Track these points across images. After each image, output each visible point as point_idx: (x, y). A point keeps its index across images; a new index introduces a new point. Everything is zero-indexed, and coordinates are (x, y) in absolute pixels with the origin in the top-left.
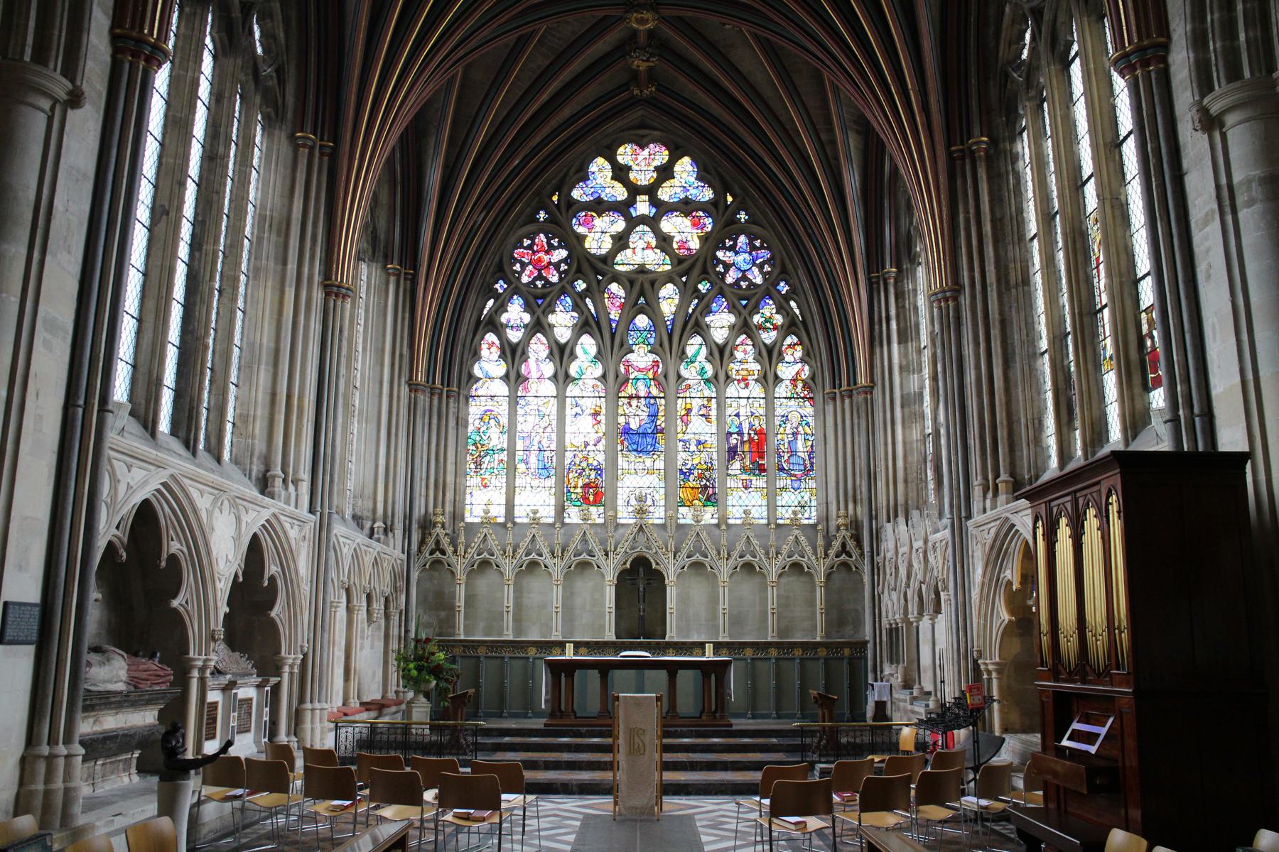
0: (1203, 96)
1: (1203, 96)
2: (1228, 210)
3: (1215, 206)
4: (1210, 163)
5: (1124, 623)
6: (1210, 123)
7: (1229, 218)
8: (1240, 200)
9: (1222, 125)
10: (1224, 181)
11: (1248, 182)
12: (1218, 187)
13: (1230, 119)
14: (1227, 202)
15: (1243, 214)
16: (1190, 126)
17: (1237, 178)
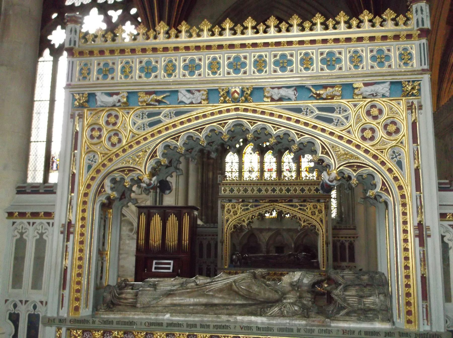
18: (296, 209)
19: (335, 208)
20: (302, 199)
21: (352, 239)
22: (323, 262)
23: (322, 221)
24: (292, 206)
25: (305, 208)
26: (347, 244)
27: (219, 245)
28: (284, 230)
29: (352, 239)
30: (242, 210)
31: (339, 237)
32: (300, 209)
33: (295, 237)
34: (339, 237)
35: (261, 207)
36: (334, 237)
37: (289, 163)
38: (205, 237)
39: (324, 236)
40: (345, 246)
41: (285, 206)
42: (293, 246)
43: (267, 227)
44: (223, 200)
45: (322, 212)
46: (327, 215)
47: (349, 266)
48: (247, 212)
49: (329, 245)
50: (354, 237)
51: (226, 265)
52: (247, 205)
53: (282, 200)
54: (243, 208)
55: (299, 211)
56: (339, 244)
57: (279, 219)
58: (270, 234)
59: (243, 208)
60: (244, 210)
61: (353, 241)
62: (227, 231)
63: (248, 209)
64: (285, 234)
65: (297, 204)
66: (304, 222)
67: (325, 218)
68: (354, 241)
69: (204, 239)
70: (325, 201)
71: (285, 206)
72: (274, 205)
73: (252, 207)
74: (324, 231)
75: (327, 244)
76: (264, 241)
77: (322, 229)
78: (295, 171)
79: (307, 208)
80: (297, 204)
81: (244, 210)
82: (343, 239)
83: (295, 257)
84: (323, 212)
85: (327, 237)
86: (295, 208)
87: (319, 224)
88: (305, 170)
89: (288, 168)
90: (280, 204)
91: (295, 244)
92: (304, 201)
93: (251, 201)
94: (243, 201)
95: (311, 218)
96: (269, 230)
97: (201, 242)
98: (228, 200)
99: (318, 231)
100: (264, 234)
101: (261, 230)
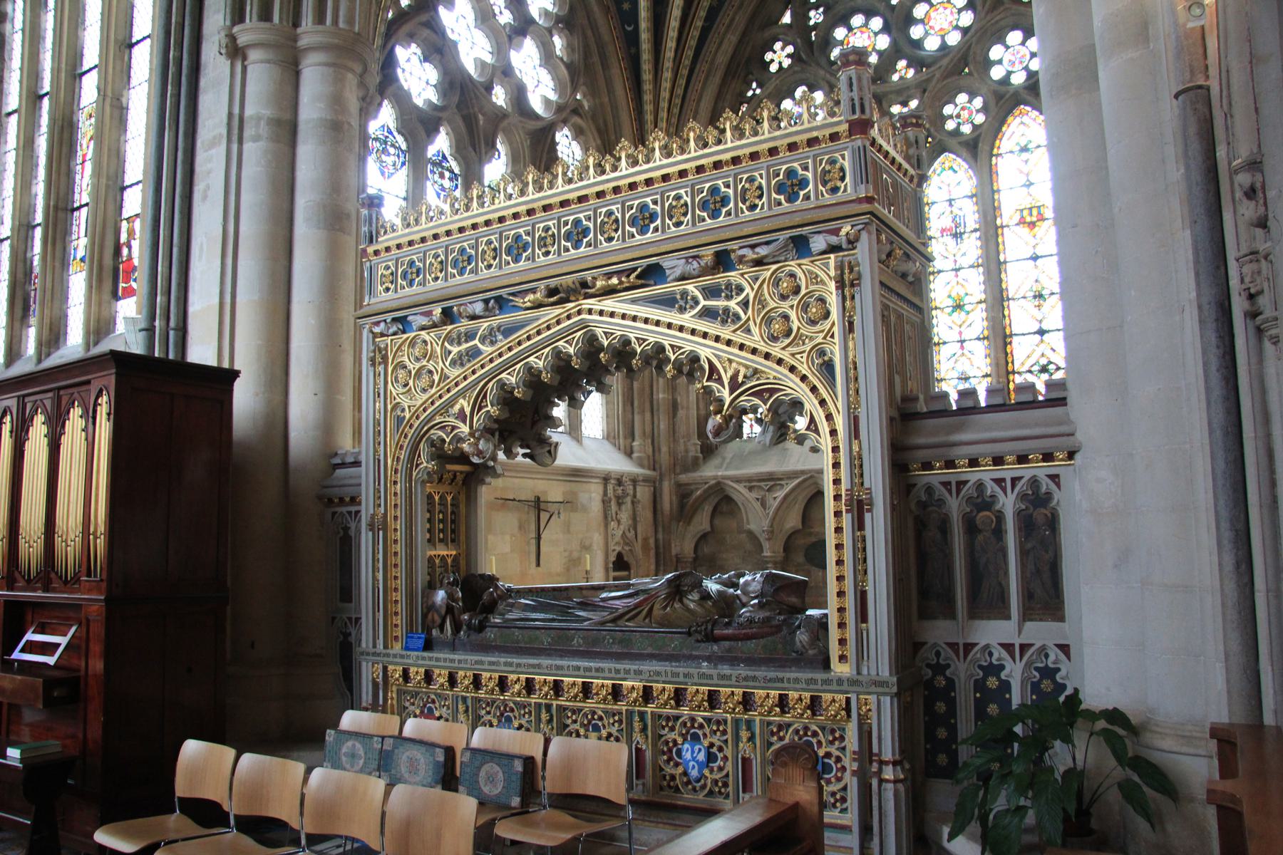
0: (234, 24)
1: (234, 24)
2: (235, 138)
3: (225, 132)
4: (227, 89)
5: (102, 528)
6: (235, 52)
7: (235, 147)
8: (248, 133)
9: (244, 58)
10: (236, 111)
11: (259, 118)
12: (230, 115)
13: (253, 55)
14: (236, 131)
15: (247, 146)
16: (216, 48)
17: (249, 112)
18: (687, 319)
19: (980, 302)
20: (708, 254)
21: (1039, 470)
23: (828, 367)
24: (667, 302)
25: (733, 304)
26: (1008, 504)
27: (366, 538)
29: (1039, 470)
30: (453, 363)
31: (950, 464)
32: (708, 314)
37: (950, 201)
40: (1000, 517)
41: (632, 310)
44: (377, 324)
45: (827, 315)
47: (1024, 648)
50: (1048, 457)
52: (470, 336)
53: (609, 276)
55: (702, 326)
59: (455, 350)
61: (1046, 484)
65: (691, 288)
66: (734, 385)
68: (1054, 478)
69: (350, 513)
70: (834, 240)
71: (632, 310)
72: (579, 312)
73: (489, 338)
74: (840, 422)
78: (975, 230)
80: (691, 288)
81: (459, 361)
82: (986, 473)
84: (835, 315)
85: (857, 464)
86: (682, 310)
88: (1017, 218)
89: (947, 222)
90: (609, 304)
92: (723, 261)
93: (478, 308)
94: (448, 316)
95: (767, 356)
97: (346, 529)
98: (394, 320)
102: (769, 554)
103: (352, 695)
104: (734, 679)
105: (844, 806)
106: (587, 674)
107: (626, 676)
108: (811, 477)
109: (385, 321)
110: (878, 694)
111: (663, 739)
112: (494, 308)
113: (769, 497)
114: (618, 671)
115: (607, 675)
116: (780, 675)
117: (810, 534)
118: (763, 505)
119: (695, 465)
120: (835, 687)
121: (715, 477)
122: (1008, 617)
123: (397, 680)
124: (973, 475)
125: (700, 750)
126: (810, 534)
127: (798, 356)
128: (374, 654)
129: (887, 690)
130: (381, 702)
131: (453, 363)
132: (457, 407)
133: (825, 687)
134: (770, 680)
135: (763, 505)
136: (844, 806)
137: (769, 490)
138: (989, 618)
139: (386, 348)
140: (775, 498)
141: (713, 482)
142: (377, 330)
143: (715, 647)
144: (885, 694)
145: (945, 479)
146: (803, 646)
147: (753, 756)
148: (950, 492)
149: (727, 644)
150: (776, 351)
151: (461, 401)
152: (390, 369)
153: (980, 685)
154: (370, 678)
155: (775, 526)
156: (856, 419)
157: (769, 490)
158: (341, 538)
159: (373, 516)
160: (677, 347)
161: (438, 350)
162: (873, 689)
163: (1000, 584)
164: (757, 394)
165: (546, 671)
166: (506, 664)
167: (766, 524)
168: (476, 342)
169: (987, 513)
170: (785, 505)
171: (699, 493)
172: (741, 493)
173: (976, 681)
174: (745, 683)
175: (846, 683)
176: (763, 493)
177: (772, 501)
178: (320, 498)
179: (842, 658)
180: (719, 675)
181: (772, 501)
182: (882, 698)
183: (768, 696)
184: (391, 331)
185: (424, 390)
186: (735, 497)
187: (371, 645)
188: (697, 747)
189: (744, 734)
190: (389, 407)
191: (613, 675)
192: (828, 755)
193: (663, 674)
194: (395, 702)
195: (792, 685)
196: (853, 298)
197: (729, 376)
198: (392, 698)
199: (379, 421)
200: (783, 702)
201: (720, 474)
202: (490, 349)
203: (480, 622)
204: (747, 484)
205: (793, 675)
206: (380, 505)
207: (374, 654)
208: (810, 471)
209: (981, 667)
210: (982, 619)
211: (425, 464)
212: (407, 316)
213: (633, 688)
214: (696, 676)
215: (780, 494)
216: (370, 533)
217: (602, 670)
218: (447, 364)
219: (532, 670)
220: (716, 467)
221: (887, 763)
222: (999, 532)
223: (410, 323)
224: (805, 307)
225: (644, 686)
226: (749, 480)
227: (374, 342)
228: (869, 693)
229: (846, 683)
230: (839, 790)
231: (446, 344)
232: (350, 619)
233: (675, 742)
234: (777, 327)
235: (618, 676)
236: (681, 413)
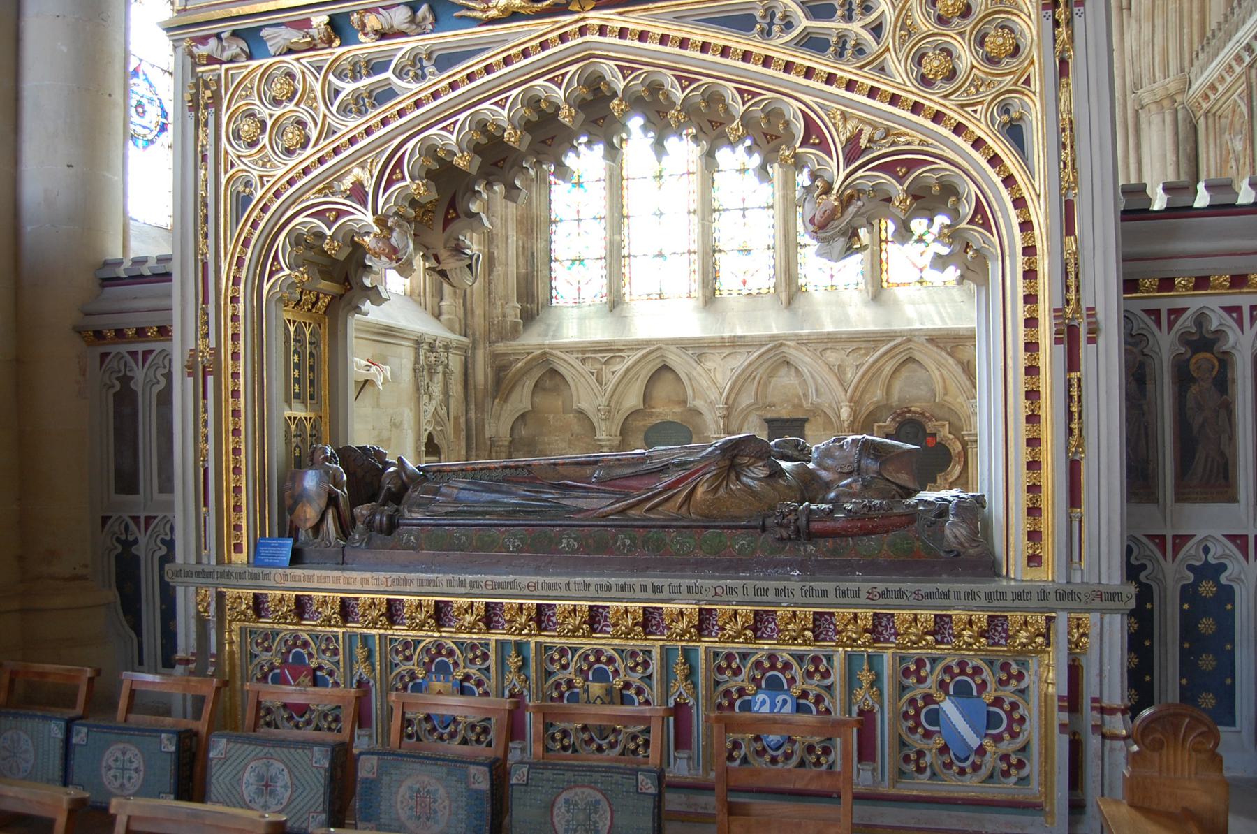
18: (778, 47)
22: (1034, 511)
27: (183, 390)
28: (802, 342)
32: (812, 43)
33: (852, 376)
34: (1167, 284)
35: (476, 64)
36: (1130, 285)
38: (141, 347)
39: (1044, 266)
40: (1225, 361)
42: (845, 413)
43: (727, 334)
44: (203, 40)
46: (1063, 68)
48: (373, 117)
49: (1086, 350)
51: (238, 548)
52: (375, 66)
54: (348, 87)
55: (804, 59)
56: (1166, 344)
57: (783, 296)
58: (740, 361)
59: (348, 87)
60: (357, 105)
62: (236, 281)
63: (384, 95)
64: (805, 359)
66: (853, 151)
67: (1053, 105)
69: (134, 354)
72: (582, 31)
73: (415, 67)
74: (1038, 213)
75: (1069, 337)
76: (713, 394)
77: (1019, 203)
79: (877, 30)
81: (357, 105)
82: (1212, 303)
83: (777, 473)
85: (1069, 275)
87: (995, 160)
91: (855, 402)
96: (735, 344)
97: (126, 380)
98: (235, 34)
99: (976, 234)
100: (709, 365)
101: (698, 349)
102: (604, 437)
103: (139, 633)
104: (863, 595)
105: (1024, 773)
106: (603, 594)
107: (673, 596)
108: (660, 348)
109: (218, 36)
110: (1103, 612)
111: (722, 688)
112: (424, 19)
113: (607, 371)
114: (658, 589)
115: (639, 595)
116: (943, 587)
117: (651, 415)
118: (600, 381)
119: (514, 332)
120: (1034, 603)
121: (541, 346)
122: (1234, 499)
123: (243, 613)
124: (1195, 303)
125: (785, 702)
126: (651, 415)
127: (969, 109)
128: (200, 574)
129: (1120, 605)
130: (214, 650)
131: (344, 110)
132: (347, 183)
133: (1018, 603)
134: (926, 596)
135: (600, 381)
136: (1024, 773)
137: (606, 363)
138: (1205, 500)
139: (218, 81)
140: (613, 372)
141: (538, 352)
142: (202, 50)
143: (811, 547)
144: (1112, 611)
145: (1152, 305)
146: (961, 544)
147: (877, 708)
148: (1158, 323)
149: (830, 543)
150: (932, 101)
151: (357, 171)
152: (224, 119)
153: (1188, 593)
154: (193, 612)
155: (613, 404)
156: (1069, 206)
157: (606, 363)
158: (115, 394)
159: (194, 352)
160: (749, 92)
161: (317, 87)
162: (1097, 604)
163: (1222, 454)
164: (887, 168)
165: (527, 592)
166: (451, 583)
167: (602, 402)
168: (389, 74)
169: (1208, 355)
170: (625, 381)
171: (520, 364)
172: (570, 368)
173: (1184, 587)
174: (882, 601)
175: (1052, 597)
176: (598, 366)
177: (609, 376)
178: (79, 331)
179: (1034, 560)
180: (837, 589)
181: (609, 376)
182: (1107, 617)
183: (915, 619)
184: (227, 55)
185: (289, 152)
186: (562, 370)
187: (193, 560)
188: (780, 698)
189: (865, 676)
190: (224, 179)
191: (650, 595)
192: (998, 701)
193: (740, 591)
194: (235, 648)
195: (963, 602)
196: (1069, 22)
197: (843, 138)
198: (231, 642)
199: (204, 199)
200: (941, 627)
201: (547, 342)
202: (415, 87)
203: (391, 518)
204: (580, 355)
205: (963, 587)
206: (207, 335)
207: (200, 574)
208: (658, 341)
209: (1191, 568)
210: (1195, 501)
211: (287, 271)
212: (260, 28)
213: (681, 613)
214: (797, 593)
215: (620, 368)
216: (191, 380)
217: (630, 588)
218: (334, 109)
219: (501, 591)
220: (539, 335)
221: (1112, 711)
222: (1223, 382)
223: (262, 41)
224: (919, 59)
225: (701, 610)
226: (584, 352)
227: (194, 73)
228: (1088, 611)
229: (1052, 597)
230: (1015, 752)
231: (331, 77)
232: (136, 519)
233: (741, 691)
234: (933, 64)
235: (659, 596)
236: (499, 269)
